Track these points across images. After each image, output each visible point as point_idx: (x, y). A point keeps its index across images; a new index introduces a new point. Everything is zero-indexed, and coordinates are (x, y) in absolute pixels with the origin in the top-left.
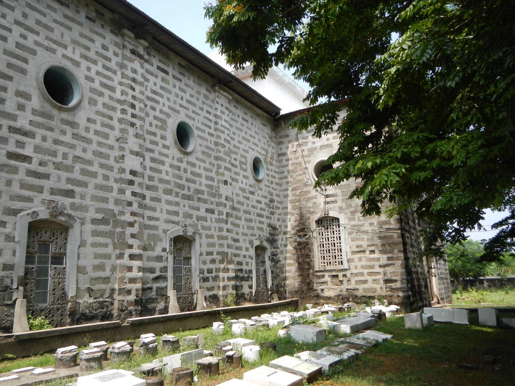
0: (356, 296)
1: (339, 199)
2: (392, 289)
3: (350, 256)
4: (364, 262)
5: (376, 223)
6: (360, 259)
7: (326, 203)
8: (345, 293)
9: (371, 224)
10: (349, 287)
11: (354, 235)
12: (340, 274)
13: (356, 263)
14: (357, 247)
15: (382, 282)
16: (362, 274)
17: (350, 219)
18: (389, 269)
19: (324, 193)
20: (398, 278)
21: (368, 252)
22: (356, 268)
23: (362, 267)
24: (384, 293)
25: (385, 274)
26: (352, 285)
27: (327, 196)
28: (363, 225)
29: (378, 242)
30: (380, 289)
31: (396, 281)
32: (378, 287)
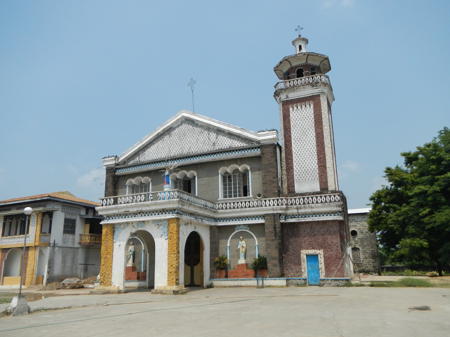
0: (365, 271)
1: (359, 242)
2: (375, 269)
3: (363, 259)
4: (367, 261)
5: (370, 250)
6: (366, 260)
7: (355, 243)
8: (361, 270)
9: (369, 251)
10: (363, 268)
11: (364, 253)
12: (360, 265)
13: (365, 261)
14: (365, 257)
15: (373, 267)
16: (367, 265)
17: (363, 249)
18: (375, 264)
19: (354, 240)
20: (377, 266)
21: (368, 259)
22: (365, 263)
23: (367, 263)
24: (373, 270)
25: (373, 265)
26: (364, 268)
27: (355, 241)
28: (367, 251)
29: (371, 256)
30: (372, 269)
31: (377, 267)
32: (371, 268)
